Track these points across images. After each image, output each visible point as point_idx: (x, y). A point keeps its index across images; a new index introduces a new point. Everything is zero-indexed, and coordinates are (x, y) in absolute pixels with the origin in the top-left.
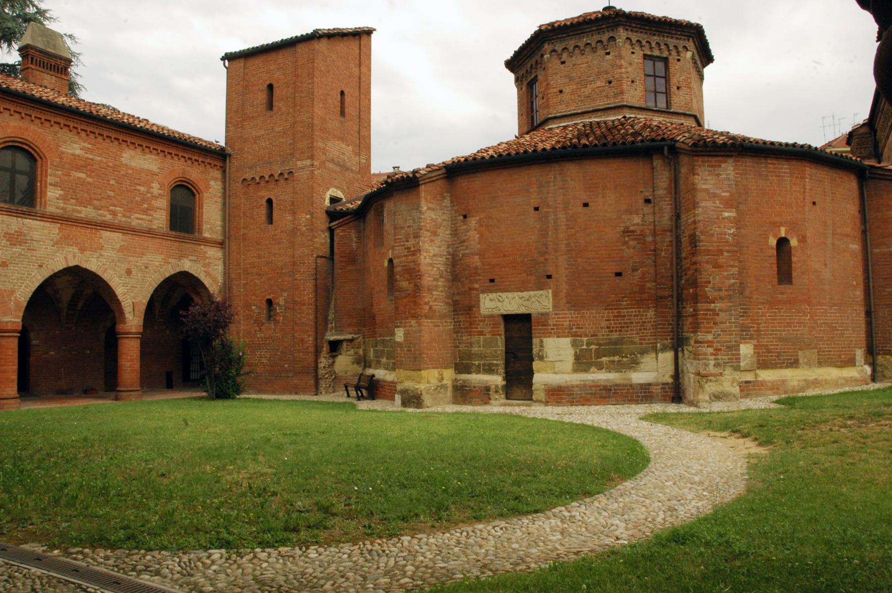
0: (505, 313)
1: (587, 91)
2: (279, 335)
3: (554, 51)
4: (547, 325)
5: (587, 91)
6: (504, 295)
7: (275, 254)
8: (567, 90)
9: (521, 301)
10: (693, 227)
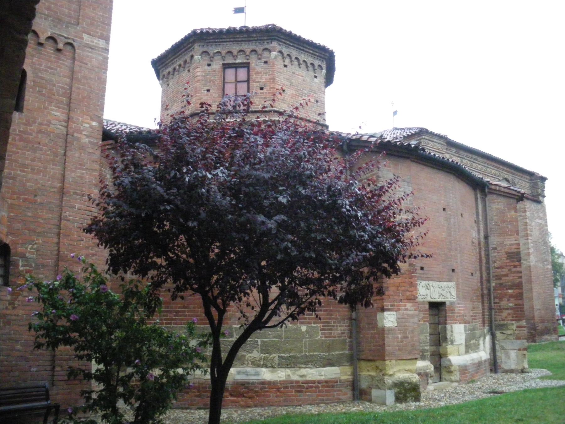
0: (432, 300)
2: (21, 312)
4: (454, 313)
6: (431, 283)
7: (26, 166)
9: (440, 291)
10: (514, 247)
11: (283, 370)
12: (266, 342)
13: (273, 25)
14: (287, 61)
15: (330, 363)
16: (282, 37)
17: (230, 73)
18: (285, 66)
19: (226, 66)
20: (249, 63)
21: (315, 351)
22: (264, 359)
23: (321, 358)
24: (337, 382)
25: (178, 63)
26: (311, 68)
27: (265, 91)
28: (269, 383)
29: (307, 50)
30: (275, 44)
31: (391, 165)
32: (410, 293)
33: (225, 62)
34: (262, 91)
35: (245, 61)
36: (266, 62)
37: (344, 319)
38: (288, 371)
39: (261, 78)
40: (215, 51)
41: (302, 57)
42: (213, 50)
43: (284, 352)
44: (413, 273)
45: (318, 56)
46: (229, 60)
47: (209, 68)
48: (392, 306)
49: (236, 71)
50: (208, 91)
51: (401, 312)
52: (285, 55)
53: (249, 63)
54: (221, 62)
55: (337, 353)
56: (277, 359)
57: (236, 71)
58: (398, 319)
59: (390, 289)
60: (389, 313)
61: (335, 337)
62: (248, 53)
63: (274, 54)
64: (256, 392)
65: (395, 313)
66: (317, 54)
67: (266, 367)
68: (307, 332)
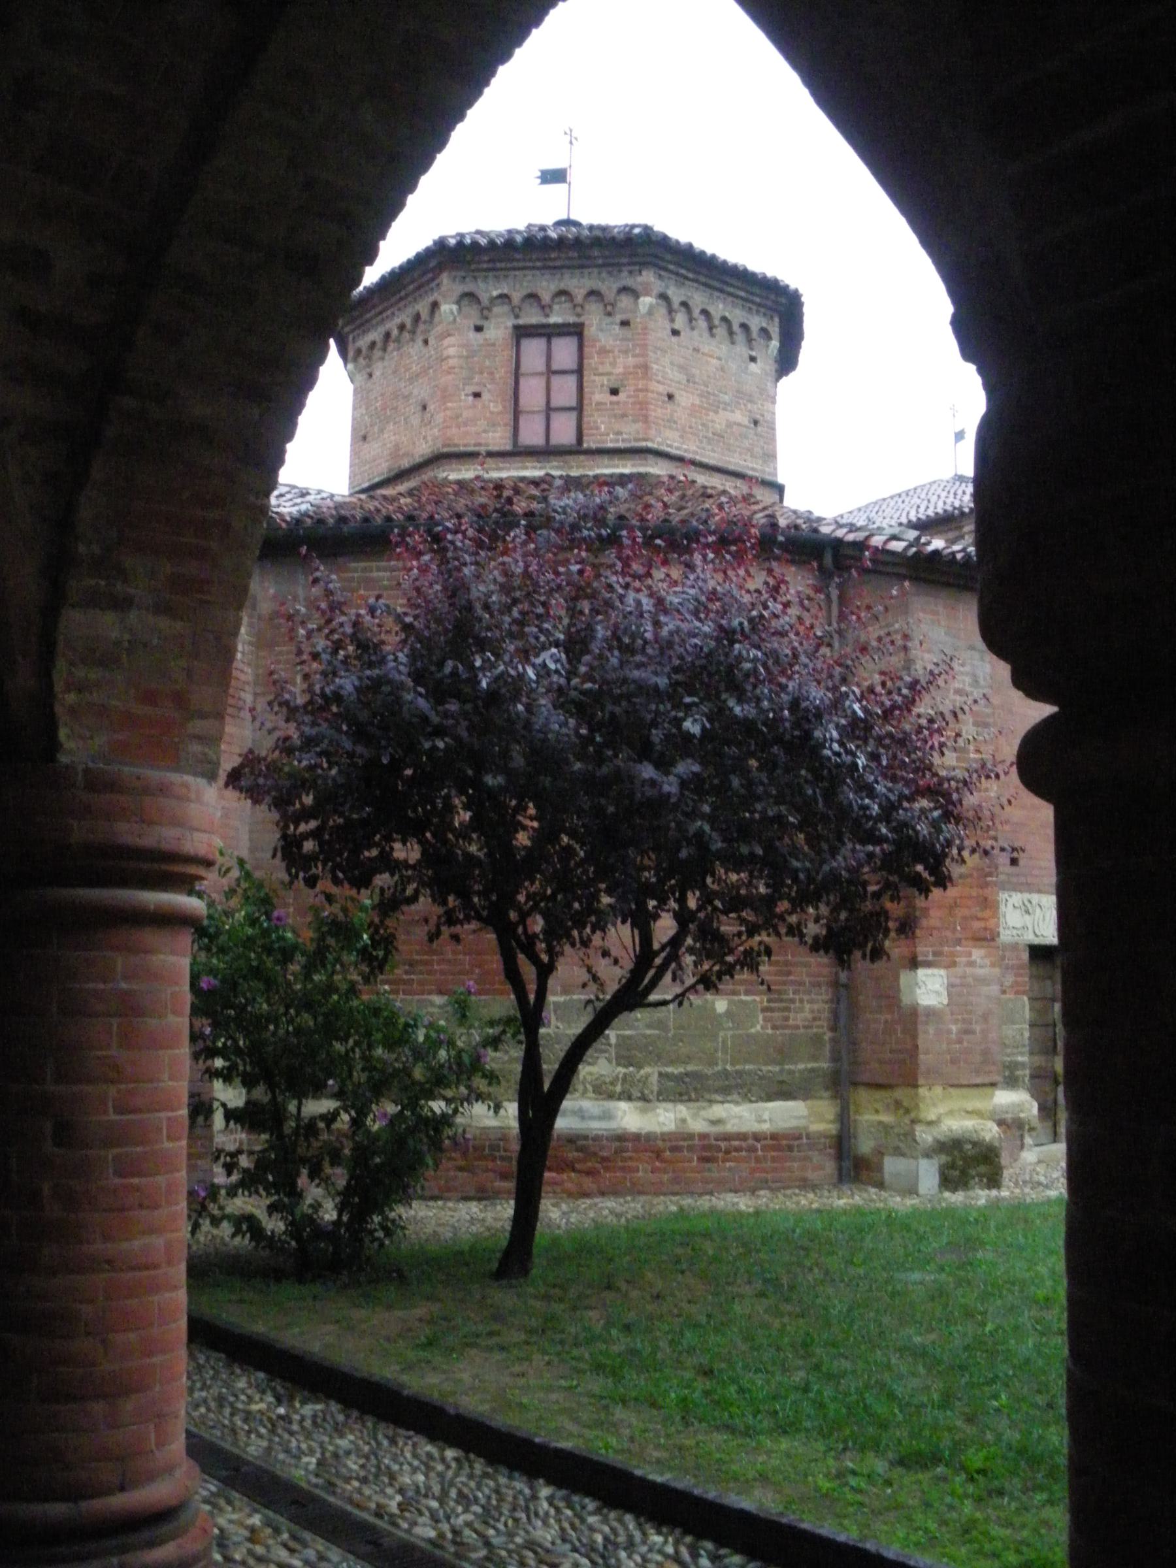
1: (720, 420)
3: (663, 297)
5: (720, 420)
6: (1035, 897)
8: (685, 399)
11: (670, 1105)
12: (630, 1037)
13: (647, 229)
14: (680, 320)
15: (783, 1092)
16: (669, 257)
17: (533, 349)
18: (675, 333)
19: (522, 333)
20: (582, 325)
21: (746, 1061)
22: (625, 1079)
23: (761, 1078)
24: (799, 1137)
25: (397, 321)
26: (740, 337)
27: (622, 396)
28: (637, 1137)
29: (731, 290)
30: (648, 276)
31: (941, 609)
32: (982, 924)
33: (521, 322)
34: (614, 398)
35: (572, 319)
36: (625, 324)
37: (819, 985)
38: (682, 1110)
39: (614, 364)
40: (495, 293)
41: (719, 308)
42: (489, 289)
43: (672, 1063)
44: (990, 875)
45: (759, 305)
46: (532, 317)
47: (479, 336)
48: (935, 954)
49: (549, 342)
50: (477, 395)
51: (959, 970)
52: (676, 305)
53: (582, 325)
54: (510, 323)
55: (801, 1066)
56: (654, 1078)
57: (549, 342)
58: (951, 986)
59: (932, 912)
60: (929, 971)
61: (797, 1027)
62: (579, 299)
63: (646, 301)
64: (605, 1159)
65: (942, 972)
66: (758, 300)
67: (630, 1098)
68: (728, 1014)
